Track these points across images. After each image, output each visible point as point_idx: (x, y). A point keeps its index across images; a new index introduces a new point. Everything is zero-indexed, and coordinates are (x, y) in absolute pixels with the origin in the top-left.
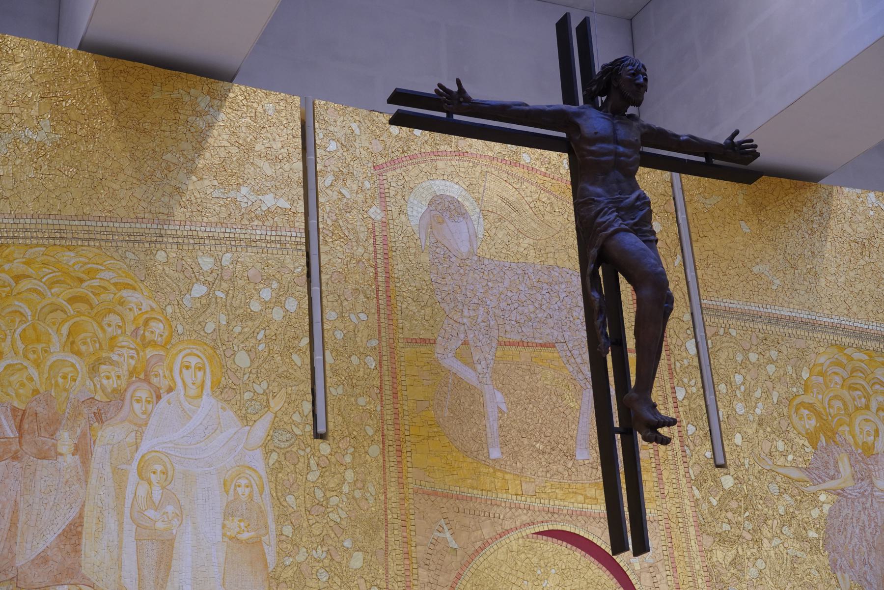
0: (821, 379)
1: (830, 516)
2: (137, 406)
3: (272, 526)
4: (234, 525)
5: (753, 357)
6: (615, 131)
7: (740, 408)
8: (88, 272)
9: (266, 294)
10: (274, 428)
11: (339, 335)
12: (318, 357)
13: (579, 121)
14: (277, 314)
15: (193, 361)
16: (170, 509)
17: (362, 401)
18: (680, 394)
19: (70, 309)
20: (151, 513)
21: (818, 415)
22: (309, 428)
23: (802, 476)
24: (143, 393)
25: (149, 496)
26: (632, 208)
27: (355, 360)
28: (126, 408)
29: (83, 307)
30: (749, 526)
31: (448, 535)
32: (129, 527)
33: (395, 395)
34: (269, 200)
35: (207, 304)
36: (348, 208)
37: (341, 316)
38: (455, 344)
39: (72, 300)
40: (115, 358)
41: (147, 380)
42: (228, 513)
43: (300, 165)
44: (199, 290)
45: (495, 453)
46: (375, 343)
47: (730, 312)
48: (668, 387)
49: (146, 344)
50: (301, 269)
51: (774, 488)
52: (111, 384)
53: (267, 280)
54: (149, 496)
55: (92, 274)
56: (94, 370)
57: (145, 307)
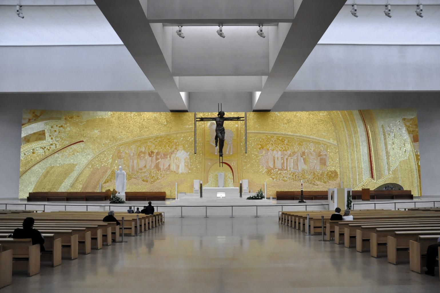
1: (261, 158)
2: (175, 152)
4: (185, 164)
5: (253, 138)
6: (220, 120)
7: (250, 146)
9: (190, 138)
10: (190, 153)
13: (216, 119)
14: (191, 140)
16: (179, 162)
17: (200, 149)
18: (242, 144)
20: (177, 163)
22: (194, 153)
25: (177, 161)
26: (221, 130)
27: (200, 144)
30: (248, 160)
31: (209, 163)
32: (175, 165)
33: (204, 148)
34: (190, 126)
35: (183, 140)
37: (198, 139)
39: (169, 142)
40: (173, 147)
41: (176, 149)
42: (185, 163)
43: (194, 121)
44: (182, 139)
46: (202, 142)
47: (250, 133)
50: (194, 134)
51: (253, 155)
53: (190, 136)
55: (171, 138)
56: (171, 149)
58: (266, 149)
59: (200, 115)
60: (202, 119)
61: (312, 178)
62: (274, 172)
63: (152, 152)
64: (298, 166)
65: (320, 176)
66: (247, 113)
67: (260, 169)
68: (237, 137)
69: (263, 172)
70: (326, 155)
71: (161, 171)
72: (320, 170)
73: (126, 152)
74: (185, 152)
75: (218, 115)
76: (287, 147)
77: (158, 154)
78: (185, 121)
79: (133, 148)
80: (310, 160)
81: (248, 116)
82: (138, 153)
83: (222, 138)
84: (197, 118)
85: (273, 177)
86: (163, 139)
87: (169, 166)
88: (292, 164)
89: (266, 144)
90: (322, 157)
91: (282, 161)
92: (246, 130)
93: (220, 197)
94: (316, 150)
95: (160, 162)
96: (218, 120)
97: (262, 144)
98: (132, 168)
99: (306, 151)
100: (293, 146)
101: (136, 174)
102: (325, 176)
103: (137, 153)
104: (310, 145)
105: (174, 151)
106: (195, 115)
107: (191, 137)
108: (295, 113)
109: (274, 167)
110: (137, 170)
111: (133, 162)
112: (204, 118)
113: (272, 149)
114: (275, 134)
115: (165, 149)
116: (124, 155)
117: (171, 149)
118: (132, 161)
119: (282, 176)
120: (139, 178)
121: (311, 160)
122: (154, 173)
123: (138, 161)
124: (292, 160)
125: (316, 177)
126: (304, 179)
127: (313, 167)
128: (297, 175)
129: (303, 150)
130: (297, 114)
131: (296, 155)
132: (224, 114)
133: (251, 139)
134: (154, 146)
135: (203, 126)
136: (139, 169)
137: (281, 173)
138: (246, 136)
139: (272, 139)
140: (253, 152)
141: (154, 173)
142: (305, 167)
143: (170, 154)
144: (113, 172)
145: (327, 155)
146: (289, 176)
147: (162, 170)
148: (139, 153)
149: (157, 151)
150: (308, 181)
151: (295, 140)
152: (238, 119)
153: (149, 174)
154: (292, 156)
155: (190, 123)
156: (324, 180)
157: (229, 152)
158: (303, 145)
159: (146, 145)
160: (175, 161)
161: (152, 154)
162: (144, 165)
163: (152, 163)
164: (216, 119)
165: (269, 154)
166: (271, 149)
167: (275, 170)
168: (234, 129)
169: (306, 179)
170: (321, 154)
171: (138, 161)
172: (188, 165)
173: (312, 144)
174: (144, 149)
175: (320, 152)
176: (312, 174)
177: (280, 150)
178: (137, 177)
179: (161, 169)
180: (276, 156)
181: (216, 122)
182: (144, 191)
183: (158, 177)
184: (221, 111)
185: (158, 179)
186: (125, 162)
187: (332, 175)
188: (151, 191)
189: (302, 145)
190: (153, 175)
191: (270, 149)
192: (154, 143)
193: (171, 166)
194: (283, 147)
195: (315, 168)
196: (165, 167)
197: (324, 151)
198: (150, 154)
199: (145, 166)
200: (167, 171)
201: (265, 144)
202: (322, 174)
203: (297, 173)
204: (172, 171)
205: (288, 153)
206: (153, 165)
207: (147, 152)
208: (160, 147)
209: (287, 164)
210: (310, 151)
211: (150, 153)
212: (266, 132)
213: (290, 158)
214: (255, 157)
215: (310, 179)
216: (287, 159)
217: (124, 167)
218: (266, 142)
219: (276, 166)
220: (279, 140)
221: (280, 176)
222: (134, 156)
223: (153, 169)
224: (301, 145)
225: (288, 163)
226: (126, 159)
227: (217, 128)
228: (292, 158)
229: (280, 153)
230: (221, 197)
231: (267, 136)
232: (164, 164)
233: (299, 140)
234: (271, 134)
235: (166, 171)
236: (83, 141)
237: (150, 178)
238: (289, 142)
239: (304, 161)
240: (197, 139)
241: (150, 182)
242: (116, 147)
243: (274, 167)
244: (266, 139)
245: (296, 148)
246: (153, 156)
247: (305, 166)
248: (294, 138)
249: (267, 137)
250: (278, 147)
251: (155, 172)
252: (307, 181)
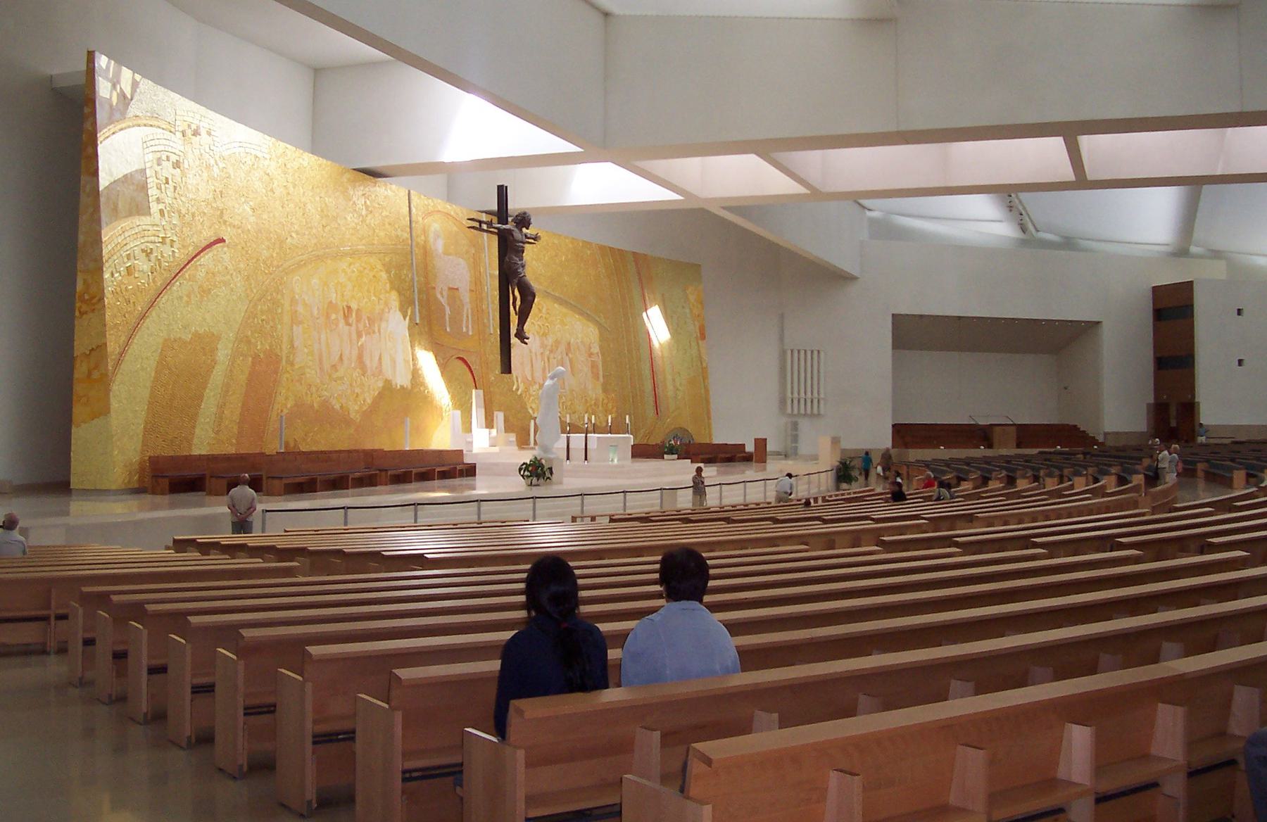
38: (440, 290)
52: (382, 307)
69: (519, 393)
85: (534, 406)
105: (383, 310)
131: (559, 349)
157: (467, 327)
177: (538, 333)
180: (533, 351)
199: (341, 358)
207: (341, 308)
213: (552, 356)
228: (556, 356)
238: (548, 313)
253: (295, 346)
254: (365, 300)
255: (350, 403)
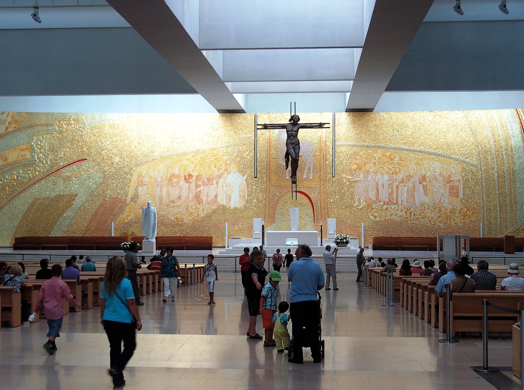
0: (360, 157)
2: (225, 176)
3: (247, 193)
6: (292, 129)
8: (217, 154)
9: (247, 153)
11: (260, 159)
12: (256, 164)
13: (287, 127)
14: (249, 157)
15: (234, 167)
16: (231, 191)
18: (327, 162)
19: (214, 160)
20: (228, 192)
21: (358, 165)
22: (254, 176)
23: (352, 178)
24: (226, 173)
25: (227, 189)
26: (294, 143)
28: (224, 176)
29: (217, 160)
32: (224, 195)
34: (248, 135)
36: (263, 135)
37: (260, 155)
41: (227, 171)
42: (240, 191)
44: (235, 154)
45: (287, 178)
48: (325, 163)
49: (226, 165)
50: (253, 148)
51: (345, 181)
52: (222, 172)
53: (247, 150)
54: (227, 189)
55: (218, 154)
56: (218, 170)
57: (227, 159)
58: (365, 170)
59: (264, 120)
60: (266, 127)
61: (437, 217)
62: (377, 207)
63: (190, 176)
64: (415, 197)
65: (448, 214)
66: (336, 114)
67: (355, 201)
68: (321, 151)
69: (360, 207)
70: (459, 181)
71: (203, 205)
72: (449, 205)
73: (150, 176)
74: (240, 175)
75: (290, 120)
76: (398, 168)
77: (198, 178)
78: (240, 128)
79: (161, 169)
80: (433, 189)
81: (338, 119)
82: (169, 176)
83: (296, 156)
84: (257, 125)
85: (375, 214)
86: (207, 155)
87: (216, 196)
88: (406, 195)
89: (365, 162)
90: (453, 184)
91: (390, 189)
92: (334, 141)
93: (291, 245)
94: (444, 172)
95: (202, 191)
96: (290, 128)
97: (359, 162)
98: (160, 199)
99: (427, 175)
100: (407, 166)
101: (165, 210)
102: (457, 215)
103: (167, 177)
104: (434, 165)
105: (222, 174)
106: (256, 117)
107: (249, 151)
108: (411, 114)
109: (377, 199)
110: (168, 204)
111: (161, 191)
112: (268, 125)
113: (374, 171)
114: (379, 147)
115: (210, 170)
116: (147, 180)
117: (218, 170)
118: (159, 189)
119: (389, 214)
120: (170, 215)
121: (436, 188)
122: (193, 208)
123: (168, 190)
124: (406, 188)
125: (443, 215)
126: (423, 218)
127: (439, 199)
128: (413, 212)
129: (423, 172)
130: (415, 116)
131: (412, 180)
132: (299, 119)
133: (342, 154)
134: (193, 165)
135: (268, 134)
136: (171, 201)
137: (388, 209)
138: (334, 151)
139: (375, 155)
140: (344, 176)
141: (193, 208)
142: (426, 200)
143: (217, 179)
144: (131, 205)
145: (461, 181)
146: (401, 214)
147: (204, 203)
148: (170, 177)
149: (197, 174)
150: (429, 221)
151: (410, 156)
152: (320, 126)
153: (186, 209)
154: (405, 182)
155: (248, 130)
156: (456, 220)
158: (423, 165)
159: (180, 165)
160: (224, 188)
161: (190, 178)
162: (179, 195)
163: (189, 193)
164: (287, 126)
165: (369, 178)
166: (372, 172)
167: (378, 204)
168: (316, 139)
169: (427, 219)
170: (452, 179)
171: (168, 190)
172: (244, 195)
173: (438, 163)
174: (178, 171)
175: (450, 177)
176: (436, 210)
177: (386, 173)
178: (167, 214)
179: (203, 202)
180: (380, 183)
181: (287, 132)
182: (178, 235)
183: (199, 213)
184: (294, 114)
185: (199, 216)
186: (149, 190)
187: (468, 212)
188: (188, 236)
189: (421, 164)
190: (191, 211)
191: (371, 170)
192: (192, 162)
193: (218, 197)
194: (392, 168)
195: (442, 201)
196: (210, 199)
197: (456, 175)
198: (186, 179)
199: (179, 197)
200: (212, 204)
201: (363, 162)
202: (453, 211)
203: (412, 209)
204: (220, 205)
205: (400, 178)
206: (191, 196)
208: (202, 168)
209: (397, 194)
210: (434, 175)
211: (187, 177)
212: (366, 144)
213: (402, 185)
214: (348, 183)
215: (432, 218)
216: (397, 187)
217: (147, 198)
218: (365, 160)
219: (380, 196)
220: (386, 156)
221: (386, 214)
222: (162, 182)
223: (191, 202)
224: (420, 165)
225: (399, 193)
226: (150, 186)
227: (289, 141)
229: (386, 177)
230: (292, 245)
231: (366, 150)
232: (208, 193)
233: (417, 157)
234: (373, 147)
235: (211, 205)
236: (87, 159)
237: (186, 215)
238: (400, 160)
239: (424, 190)
240: (258, 155)
241: (187, 221)
242: (135, 169)
243: (378, 200)
244: (364, 155)
245: (412, 169)
246: (191, 181)
247: (426, 197)
248: (410, 154)
249: (366, 153)
250: (384, 167)
251: (194, 206)
252: (428, 222)
253: (139, 194)
254: (205, 171)
255: (185, 216)
